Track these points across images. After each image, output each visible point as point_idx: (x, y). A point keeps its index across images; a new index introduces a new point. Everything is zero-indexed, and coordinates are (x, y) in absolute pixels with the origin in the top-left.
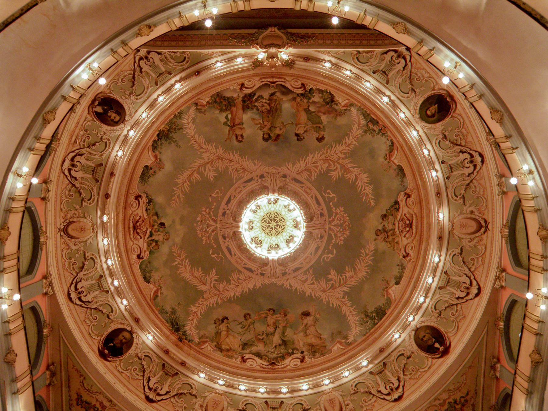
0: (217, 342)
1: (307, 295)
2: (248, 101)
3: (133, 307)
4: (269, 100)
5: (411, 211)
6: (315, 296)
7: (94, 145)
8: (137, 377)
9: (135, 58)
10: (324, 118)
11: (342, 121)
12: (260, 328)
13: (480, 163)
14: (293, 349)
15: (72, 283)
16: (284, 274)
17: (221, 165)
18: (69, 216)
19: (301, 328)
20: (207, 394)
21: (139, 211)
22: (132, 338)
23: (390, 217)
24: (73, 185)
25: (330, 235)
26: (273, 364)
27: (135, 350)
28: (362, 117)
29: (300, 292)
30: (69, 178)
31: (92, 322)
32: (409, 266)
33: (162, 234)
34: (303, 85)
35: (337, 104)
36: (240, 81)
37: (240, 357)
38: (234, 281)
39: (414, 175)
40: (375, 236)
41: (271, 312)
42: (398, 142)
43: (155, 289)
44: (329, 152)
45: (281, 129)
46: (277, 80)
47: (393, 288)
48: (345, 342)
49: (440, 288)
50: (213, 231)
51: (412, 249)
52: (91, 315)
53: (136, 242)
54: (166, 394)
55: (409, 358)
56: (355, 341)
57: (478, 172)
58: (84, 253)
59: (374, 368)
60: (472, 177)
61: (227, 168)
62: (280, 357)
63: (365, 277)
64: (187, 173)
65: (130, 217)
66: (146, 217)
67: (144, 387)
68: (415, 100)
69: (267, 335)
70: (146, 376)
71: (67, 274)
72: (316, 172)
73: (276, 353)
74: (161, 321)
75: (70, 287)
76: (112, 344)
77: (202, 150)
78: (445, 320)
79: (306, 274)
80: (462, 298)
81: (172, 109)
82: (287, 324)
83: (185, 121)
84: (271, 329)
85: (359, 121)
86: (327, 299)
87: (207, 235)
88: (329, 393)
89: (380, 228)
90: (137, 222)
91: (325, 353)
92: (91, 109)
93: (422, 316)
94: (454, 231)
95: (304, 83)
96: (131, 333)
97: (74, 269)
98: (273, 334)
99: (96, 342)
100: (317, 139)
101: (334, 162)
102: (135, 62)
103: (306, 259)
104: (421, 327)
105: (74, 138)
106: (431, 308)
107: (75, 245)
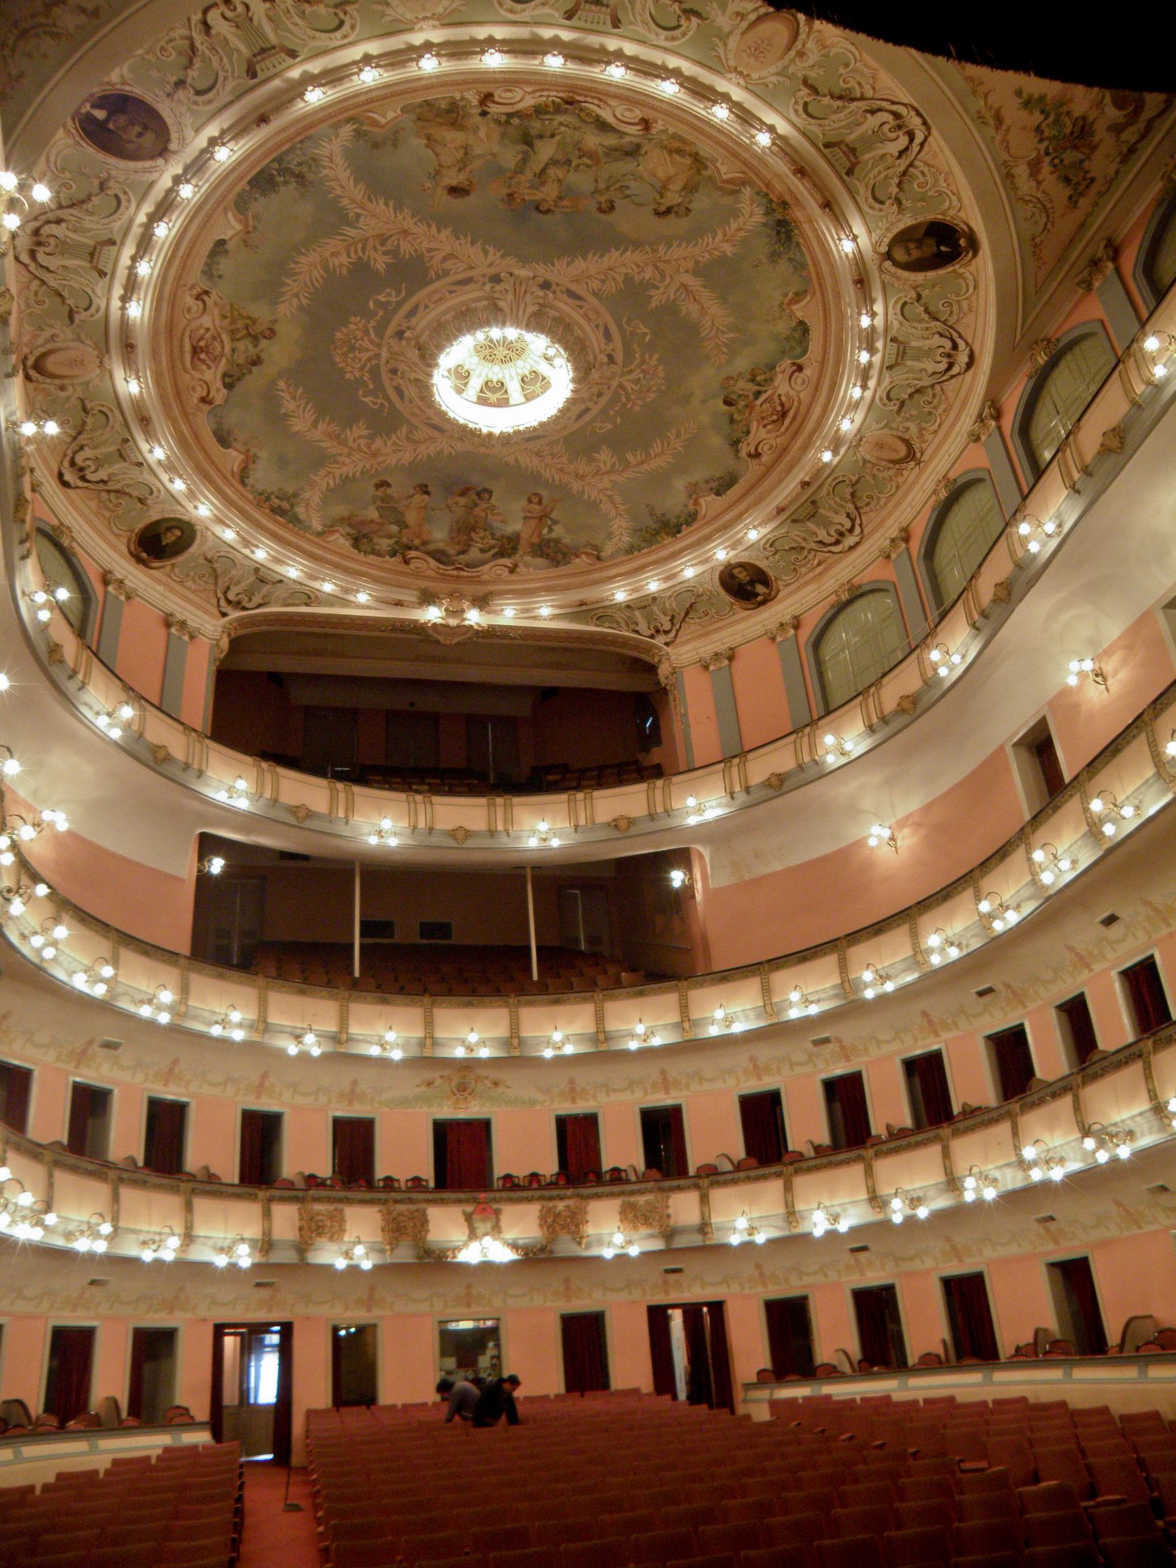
0: (699, 172)
1: (450, 229)
2: (507, 547)
3: (854, 304)
4: (469, 546)
5: (197, 375)
6: (429, 226)
7: (793, 548)
8: (926, 169)
9: (676, 636)
10: (373, 514)
11: (340, 510)
12: (581, 180)
13: (64, 471)
14: (507, 123)
15: (952, 377)
16: (496, 279)
17: (582, 466)
18: (891, 473)
19: (476, 165)
20: (774, 79)
21: (761, 435)
22: (890, 246)
23: (242, 361)
24: (857, 509)
25: (380, 335)
26: (570, 102)
27: (899, 220)
28: (302, 516)
29: (466, 236)
30: (858, 521)
31: (958, 302)
32: (195, 275)
33: (736, 389)
34: (406, 562)
35: (348, 534)
36: (513, 577)
37: (654, 131)
38: (614, 279)
39: (196, 436)
40: (277, 328)
41: (544, 207)
42: (233, 486)
43: (794, 308)
44: (368, 466)
45: (456, 503)
46: (450, 572)
47: (230, 233)
48: (362, 124)
49: (112, 242)
50: (630, 372)
51: (189, 310)
52: (951, 312)
53: (792, 393)
54: (880, 110)
55: (180, 83)
56: (337, 126)
57: (65, 455)
58: (899, 412)
59: (284, 65)
60: (75, 446)
61: (570, 461)
62: (547, 113)
63: (300, 253)
64: (653, 464)
65: (784, 433)
66: (755, 424)
67: (922, 145)
68: (205, 548)
69: (568, 162)
70: (903, 164)
71: (951, 396)
72: (398, 438)
73: (555, 123)
74: (810, 253)
75: (959, 374)
76: (943, 248)
77: (609, 493)
78: (87, 171)
79: (443, 270)
80: (48, 222)
81: (641, 562)
82: (511, 178)
83: (626, 539)
84: (553, 172)
85: (307, 511)
86: (400, 217)
87: (644, 367)
88: (425, 18)
89: (264, 343)
90: (774, 422)
91: (421, 106)
92: (773, 594)
93: (152, 184)
94: (95, 353)
95: (404, 566)
96: (888, 256)
97: (934, 396)
98: (553, 162)
99: (972, 268)
100: (389, 485)
101: (360, 450)
102: (677, 631)
103: (441, 299)
104: (153, 157)
105: (819, 570)
106: (129, 201)
107: (908, 429)
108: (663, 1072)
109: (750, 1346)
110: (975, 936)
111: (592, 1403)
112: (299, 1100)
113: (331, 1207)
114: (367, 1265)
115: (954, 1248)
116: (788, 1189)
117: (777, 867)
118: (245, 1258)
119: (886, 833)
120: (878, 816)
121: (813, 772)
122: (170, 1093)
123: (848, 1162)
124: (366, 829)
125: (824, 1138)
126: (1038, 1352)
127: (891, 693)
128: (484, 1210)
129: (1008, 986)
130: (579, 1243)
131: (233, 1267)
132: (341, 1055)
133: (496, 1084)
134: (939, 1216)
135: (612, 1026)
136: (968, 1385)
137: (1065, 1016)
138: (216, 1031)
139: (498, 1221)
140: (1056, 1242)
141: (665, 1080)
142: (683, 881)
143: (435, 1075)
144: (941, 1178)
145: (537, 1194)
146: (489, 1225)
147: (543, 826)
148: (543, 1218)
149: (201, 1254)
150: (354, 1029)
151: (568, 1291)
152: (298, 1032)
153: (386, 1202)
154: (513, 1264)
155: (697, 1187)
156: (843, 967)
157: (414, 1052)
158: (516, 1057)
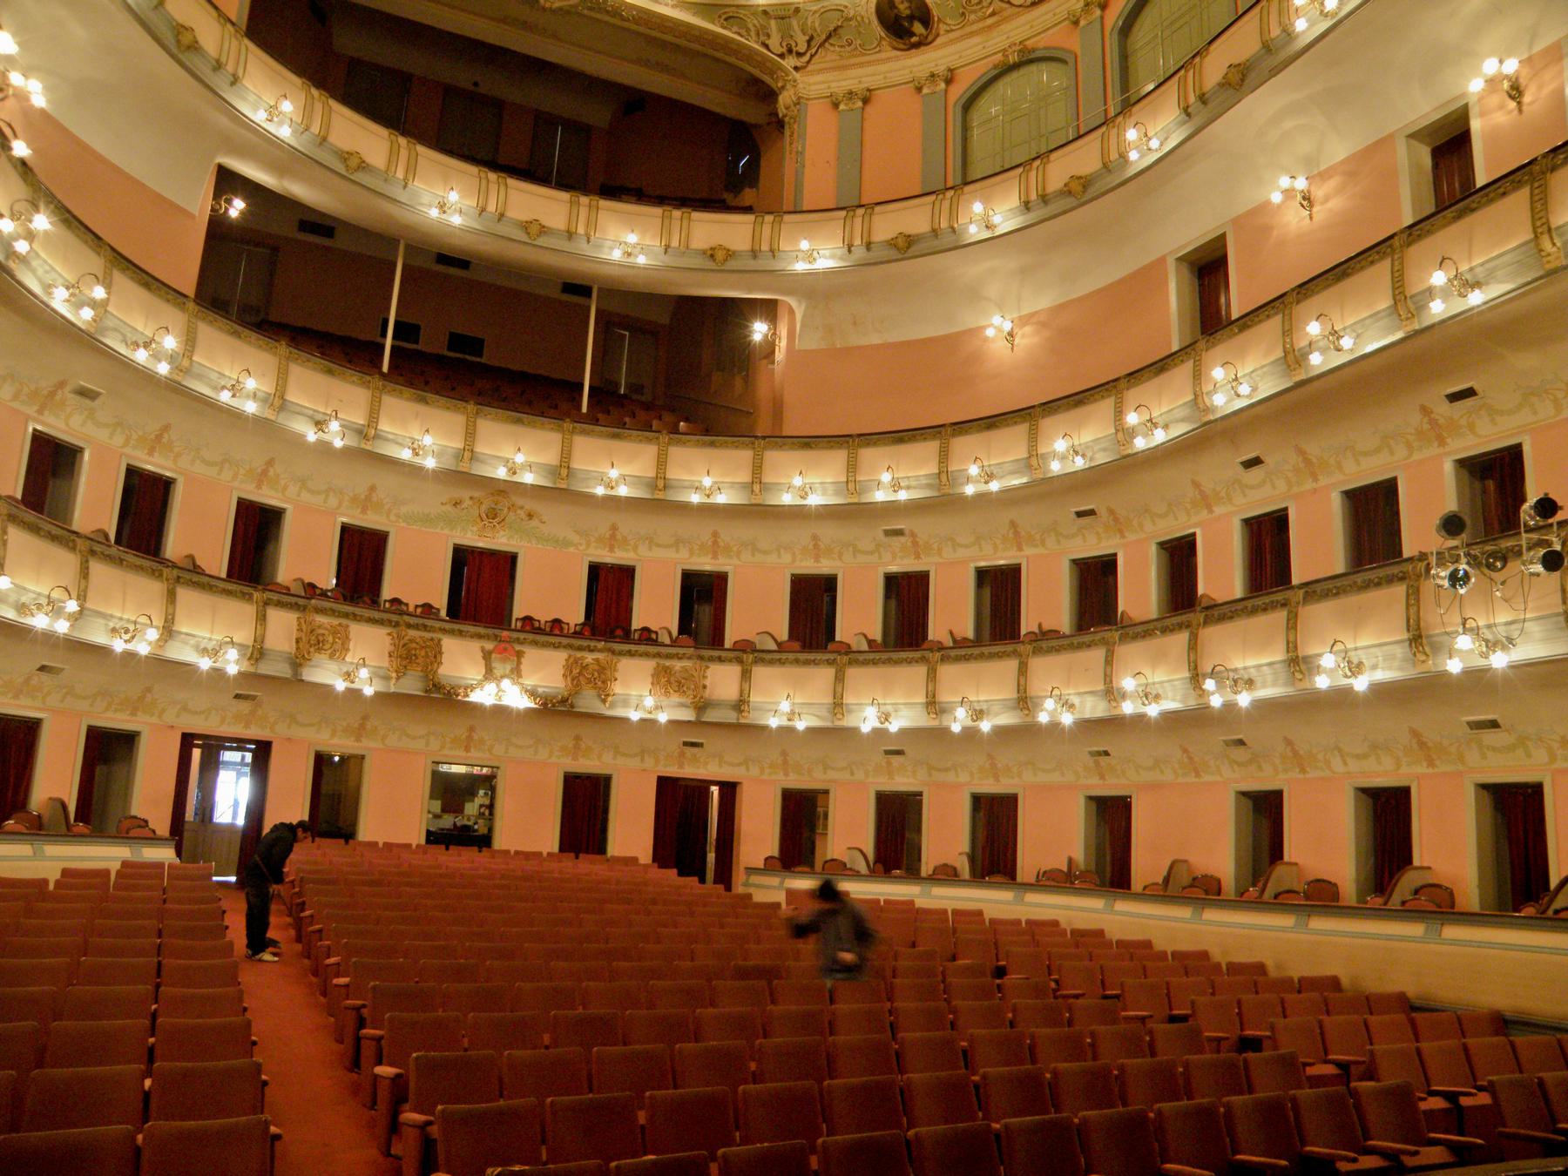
105: (990, 21)
108: (715, 535)
109: (759, 833)
110: (1104, 450)
111: (586, 866)
112: (306, 497)
113: (336, 622)
114: (369, 691)
115: (993, 766)
116: (839, 678)
117: (875, 340)
118: (232, 663)
119: (1007, 326)
120: (1001, 307)
121: (947, 240)
122: (153, 464)
123: (909, 662)
124: (426, 199)
125: (877, 633)
126: (1061, 880)
127: (1060, 171)
128: (505, 650)
129: (1111, 512)
130: (604, 701)
131: (218, 673)
132: (365, 454)
133: (530, 516)
134: (1001, 733)
135: (674, 473)
136: (994, 901)
137: (1165, 555)
138: (225, 397)
139: (519, 663)
140: (1102, 777)
141: (715, 543)
142: (766, 336)
143: (465, 494)
144: (1010, 693)
145: (565, 641)
146: (508, 667)
147: (632, 238)
148: (568, 668)
149: (181, 652)
150: (385, 426)
151: (576, 751)
152: (319, 417)
153: (397, 625)
154: (529, 711)
155: (740, 661)
156: (944, 456)
157: (449, 464)
158: (560, 490)
